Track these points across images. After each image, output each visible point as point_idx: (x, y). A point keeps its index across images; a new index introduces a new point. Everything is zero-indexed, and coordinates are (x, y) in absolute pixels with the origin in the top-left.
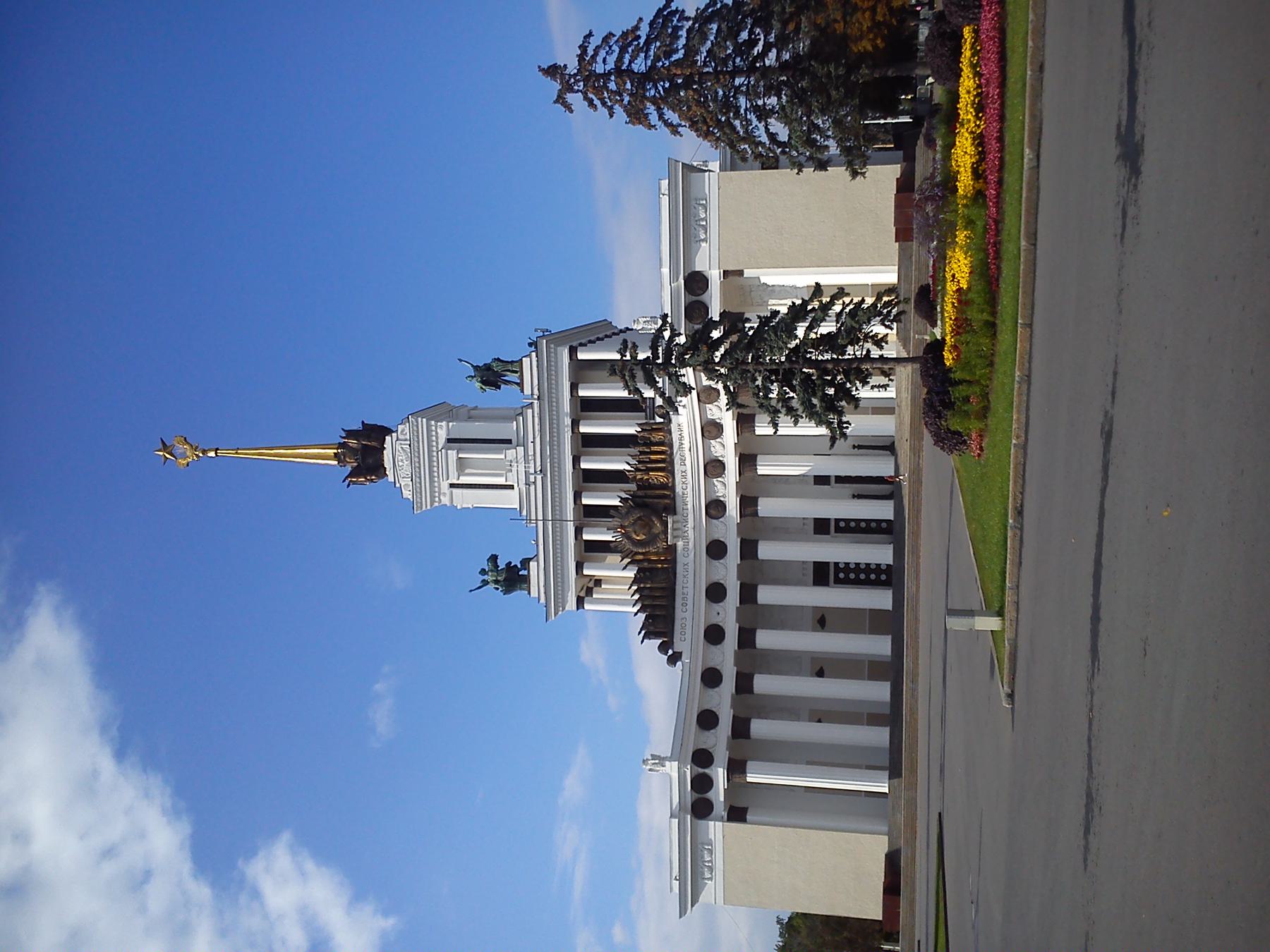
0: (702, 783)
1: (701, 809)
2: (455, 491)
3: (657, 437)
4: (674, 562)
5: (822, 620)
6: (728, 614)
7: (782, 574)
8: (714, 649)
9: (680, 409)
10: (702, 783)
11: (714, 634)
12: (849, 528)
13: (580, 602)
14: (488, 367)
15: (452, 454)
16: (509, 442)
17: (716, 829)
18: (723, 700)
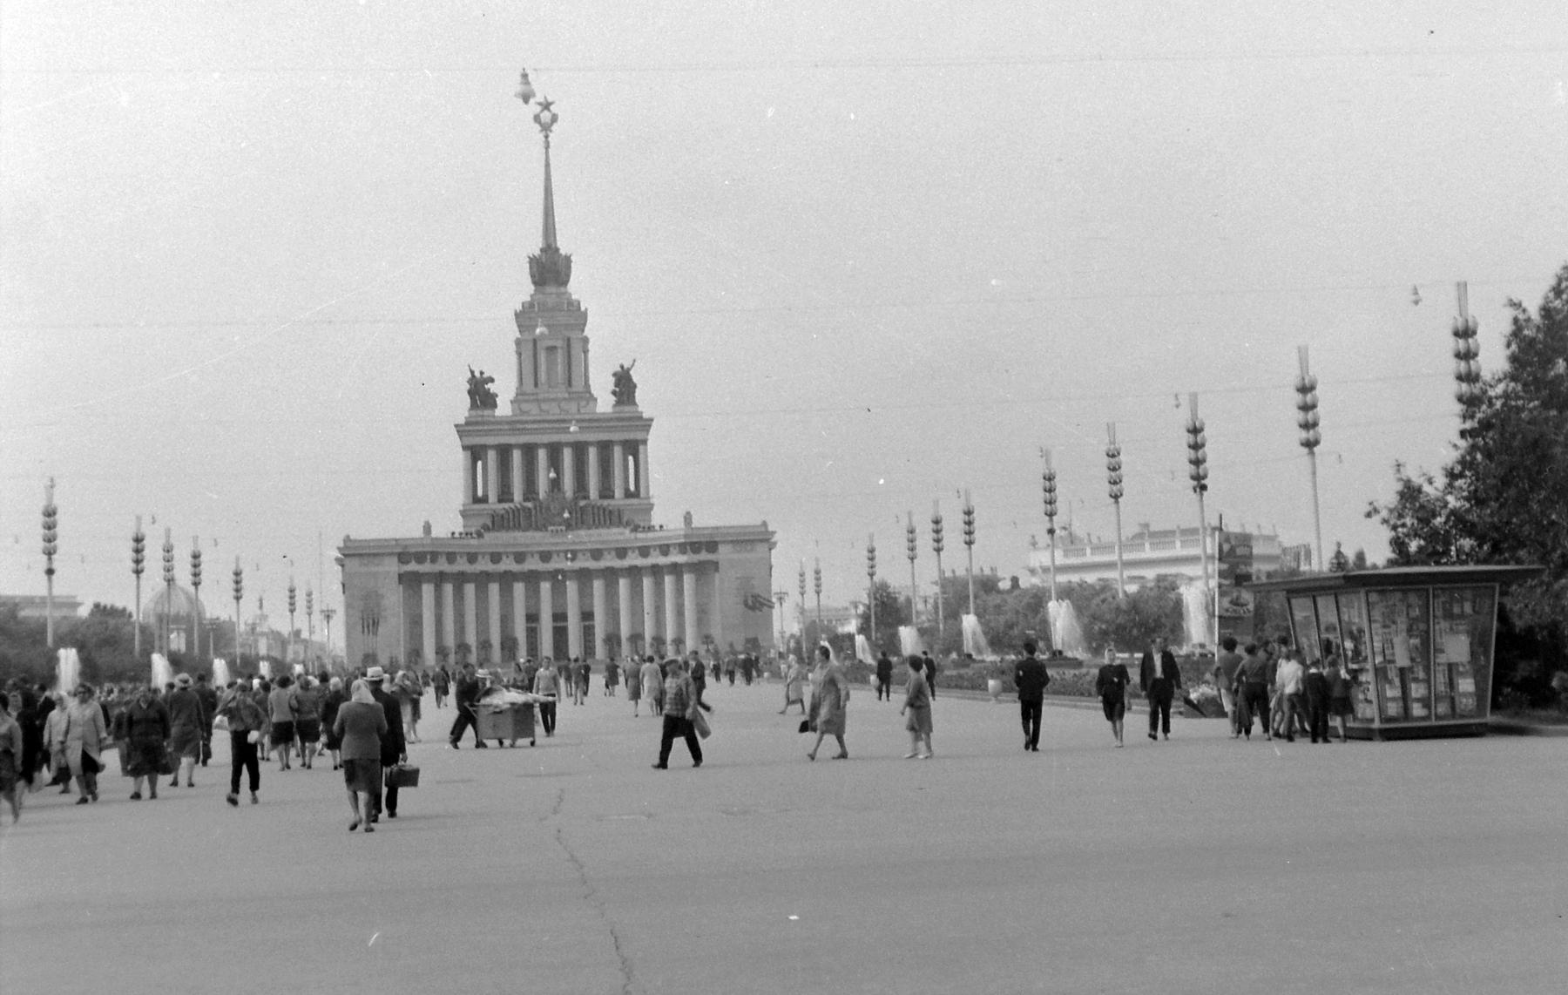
0: (420, 557)
1: (403, 557)
2: (531, 345)
3: (615, 519)
4: (537, 529)
5: (506, 620)
6: (508, 565)
7: (533, 594)
8: (488, 557)
9: (633, 536)
10: (420, 557)
11: (496, 558)
12: (560, 634)
13: (465, 448)
14: (629, 379)
15: (559, 343)
16: (570, 384)
17: (392, 567)
18: (462, 566)
